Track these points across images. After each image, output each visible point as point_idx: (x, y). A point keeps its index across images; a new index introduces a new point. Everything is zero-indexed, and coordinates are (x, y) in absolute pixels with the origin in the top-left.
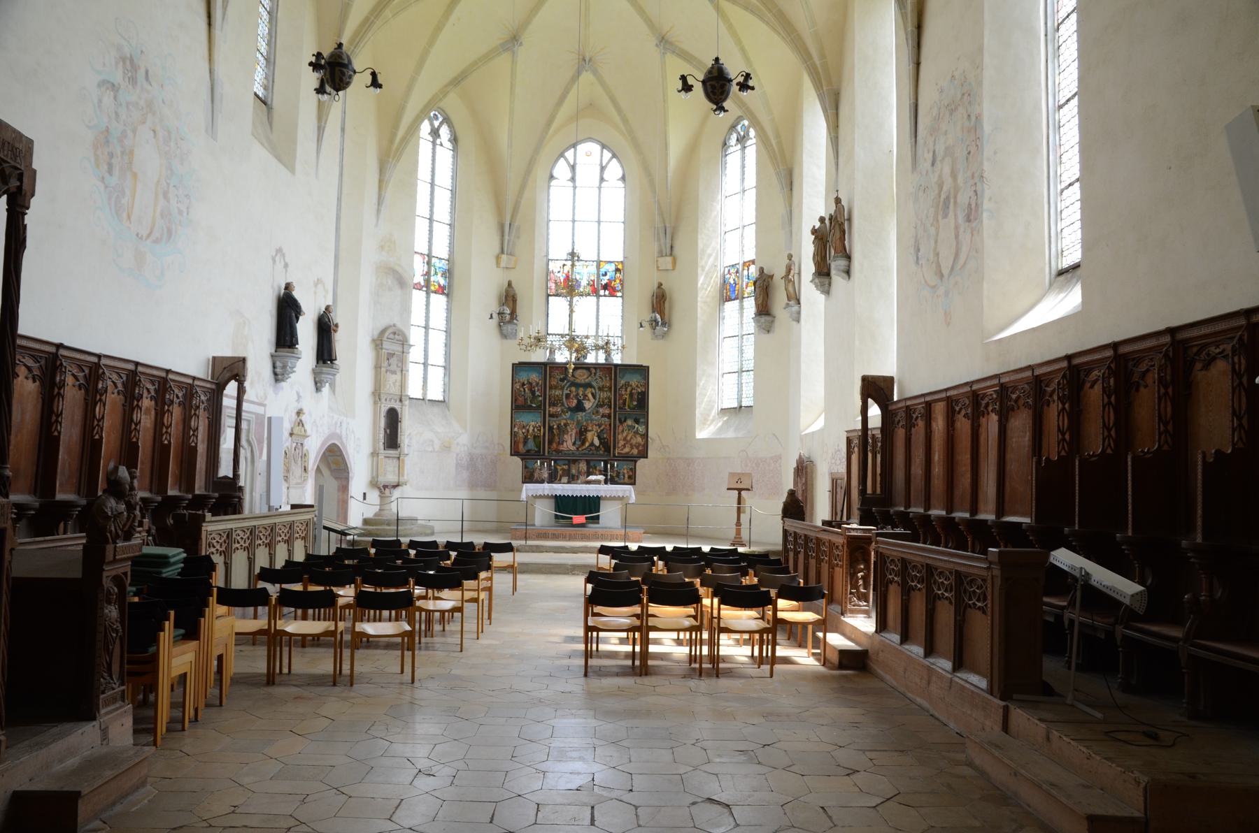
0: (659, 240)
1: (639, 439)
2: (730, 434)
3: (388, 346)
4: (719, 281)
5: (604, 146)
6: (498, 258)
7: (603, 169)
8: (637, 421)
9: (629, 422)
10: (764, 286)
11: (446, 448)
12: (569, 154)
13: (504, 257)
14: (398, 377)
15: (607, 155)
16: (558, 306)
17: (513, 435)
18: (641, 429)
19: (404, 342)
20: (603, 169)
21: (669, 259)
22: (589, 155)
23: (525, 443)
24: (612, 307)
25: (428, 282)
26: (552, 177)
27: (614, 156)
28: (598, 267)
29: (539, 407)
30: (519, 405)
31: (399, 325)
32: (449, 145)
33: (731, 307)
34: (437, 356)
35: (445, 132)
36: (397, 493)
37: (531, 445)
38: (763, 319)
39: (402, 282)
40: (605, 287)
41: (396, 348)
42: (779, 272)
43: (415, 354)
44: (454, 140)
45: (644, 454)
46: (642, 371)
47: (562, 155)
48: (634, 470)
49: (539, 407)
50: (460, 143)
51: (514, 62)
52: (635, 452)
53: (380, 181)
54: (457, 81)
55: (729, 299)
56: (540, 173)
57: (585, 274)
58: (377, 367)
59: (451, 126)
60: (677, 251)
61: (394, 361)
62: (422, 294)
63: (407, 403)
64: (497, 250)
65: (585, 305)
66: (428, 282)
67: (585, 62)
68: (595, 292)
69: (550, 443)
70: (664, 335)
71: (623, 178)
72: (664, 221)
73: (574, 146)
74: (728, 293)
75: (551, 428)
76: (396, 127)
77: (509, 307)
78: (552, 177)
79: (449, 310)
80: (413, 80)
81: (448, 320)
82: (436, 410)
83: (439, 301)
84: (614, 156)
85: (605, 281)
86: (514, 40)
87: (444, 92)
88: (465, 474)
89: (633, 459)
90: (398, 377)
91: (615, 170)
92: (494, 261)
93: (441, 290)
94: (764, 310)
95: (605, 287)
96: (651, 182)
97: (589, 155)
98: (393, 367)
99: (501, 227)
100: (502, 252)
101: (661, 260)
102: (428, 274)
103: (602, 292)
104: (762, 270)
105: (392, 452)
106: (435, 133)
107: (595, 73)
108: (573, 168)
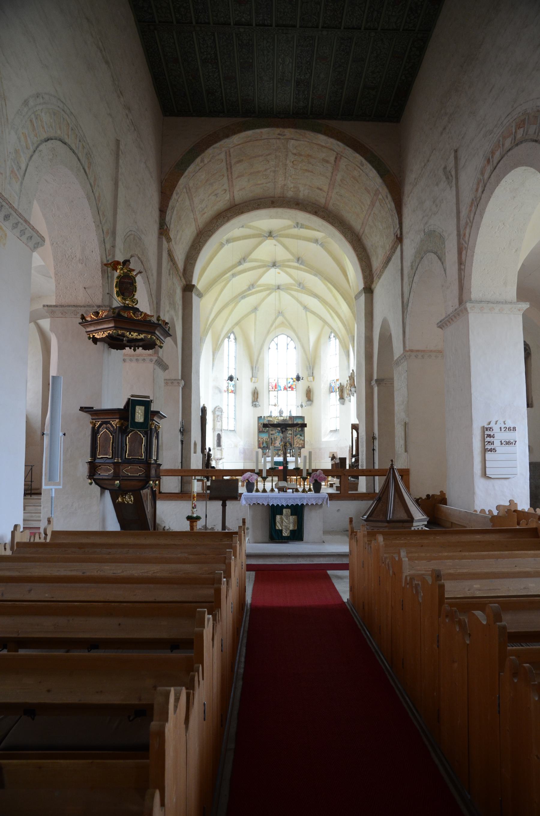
0: (307, 370)
1: (302, 442)
2: (333, 439)
3: (217, 413)
4: (329, 385)
5: (288, 336)
6: (251, 379)
7: (288, 344)
8: (301, 436)
9: (298, 436)
10: (341, 389)
11: (236, 446)
12: (275, 339)
13: (253, 378)
14: (220, 423)
15: (289, 339)
16: (273, 394)
17: (259, 441)
18: (302, 438)
19: (222, 411)
20: (288, 344)
21: (312, 378)
22: (282, 339)
23: (263, 444)
24: (292, 394)
25: (228, 389)
26: (269, 348)
27: (292, 340)
28: (287, 380)
29: (267, 432)
30: (260, 432)
31: (220, 406)
32: (234, 341)
33: (333, 394)
34: (232, 415)
35: (232, 336)
36: (221, 462)
37: (265, 445)
38: (341, 400)
39: (220, 391)
40: (290, 387)
41: (220, 413)
42: (345, 386)
43: (225, 415)
44: (235, 339)
45: (303, 447)
46: (302, 418)
47: (273, 340)
48: (300, 452)
49: (267, 432)
50: (237, 339)
51: (256, 316)
52: (300, 446)
53: (213, 359)
54: (237, 324)
55: (332, 392)
56: (265, 348)
57: (282, 384)
58: (214, 420)
59: (234, 334)
60: (314, 374)
61: (219, 418)
62: (226, 393)
63: (223, 431)
64: (251, 376)
65: (282, 393)
66: (228, 389)
67: (280, 313)
68: (285, 388)
69: (271, 444)
70: (311, 405)
71: (295, 348)
72: (309, 364)
73: (277, 337)
74: (331, 390)
75: (271, 439)
76: (218, 341)
77: (255, 396)
78: (269, 348)
79: (235, 398)
80: (223, 327)
81: (235, 402)
82: (232, 433)
83: (232, 395)
84: (292, 340)
85: (289, 385)
86: (255, 309)
87: (233, 327)
88: (242, 455)
89: (300, 449)
90: (220, 423)
91: (292, 344)
92: (250, 380)
93: (232, 392)
94: (342, 398)
95: (290, 387)
96: (305, 351)
97: (282, 339)
98: (219, 420)
99: (252, 368)
100: (253, 377)
101: (309, 378)
102: (228, 386)
103: (288, 389)
104: (341, 384)
105: (219, 448)
106: (229, 338)
107: (283, 316)
108: (277, 344)
